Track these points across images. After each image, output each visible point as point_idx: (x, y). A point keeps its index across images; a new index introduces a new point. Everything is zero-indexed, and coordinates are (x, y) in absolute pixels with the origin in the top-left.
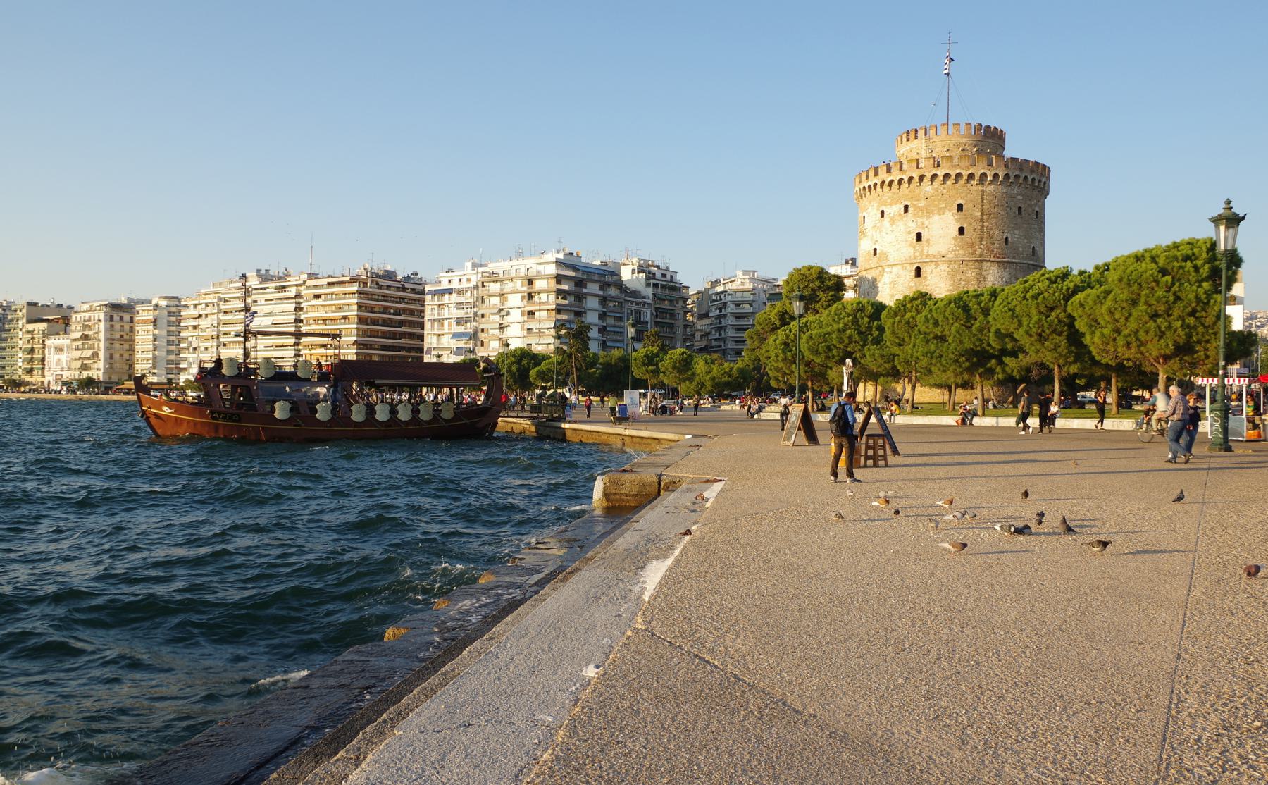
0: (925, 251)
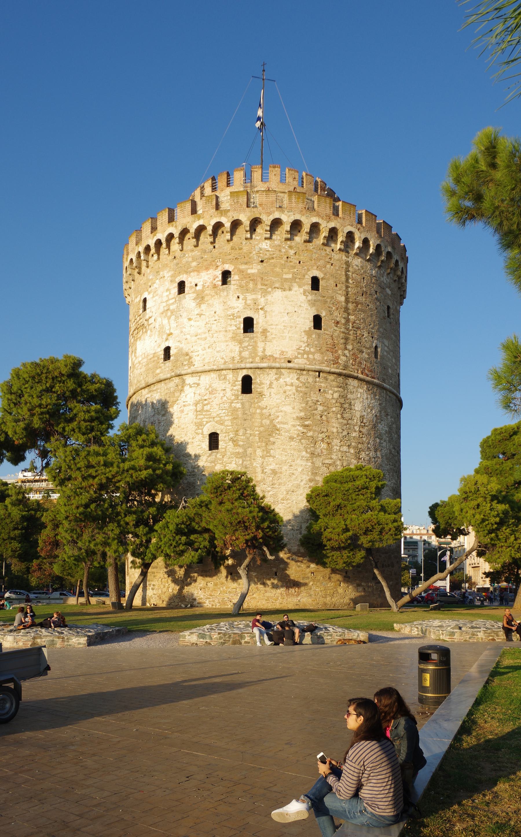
0: (260, 350)
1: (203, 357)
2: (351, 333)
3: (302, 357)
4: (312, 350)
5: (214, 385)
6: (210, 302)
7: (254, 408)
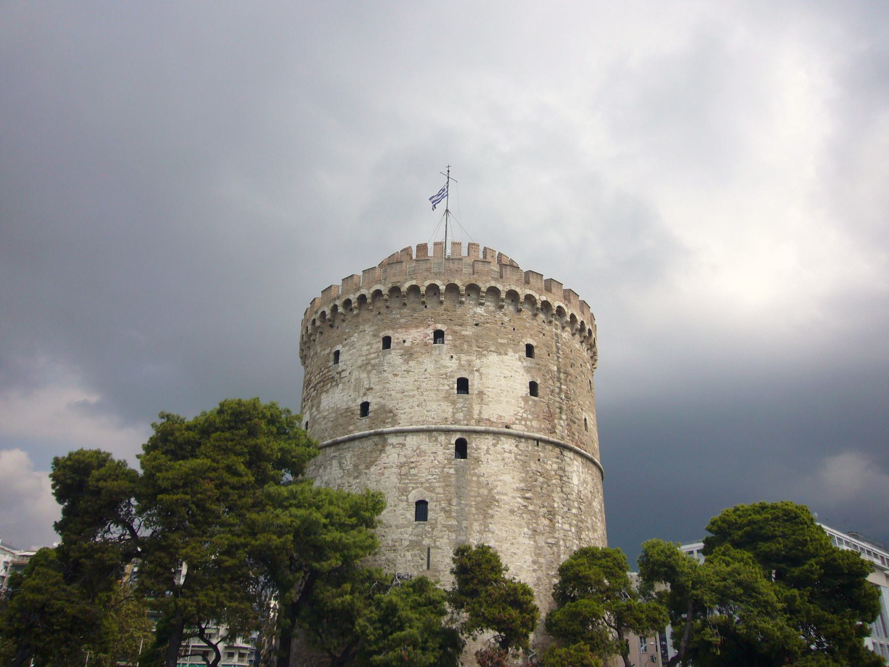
1: (412, 415)
2: (565, 402)
3: (520, 424)
4: (530, 417)
5: (423, 447)
6: (420, 359)
7: (470, 474)
